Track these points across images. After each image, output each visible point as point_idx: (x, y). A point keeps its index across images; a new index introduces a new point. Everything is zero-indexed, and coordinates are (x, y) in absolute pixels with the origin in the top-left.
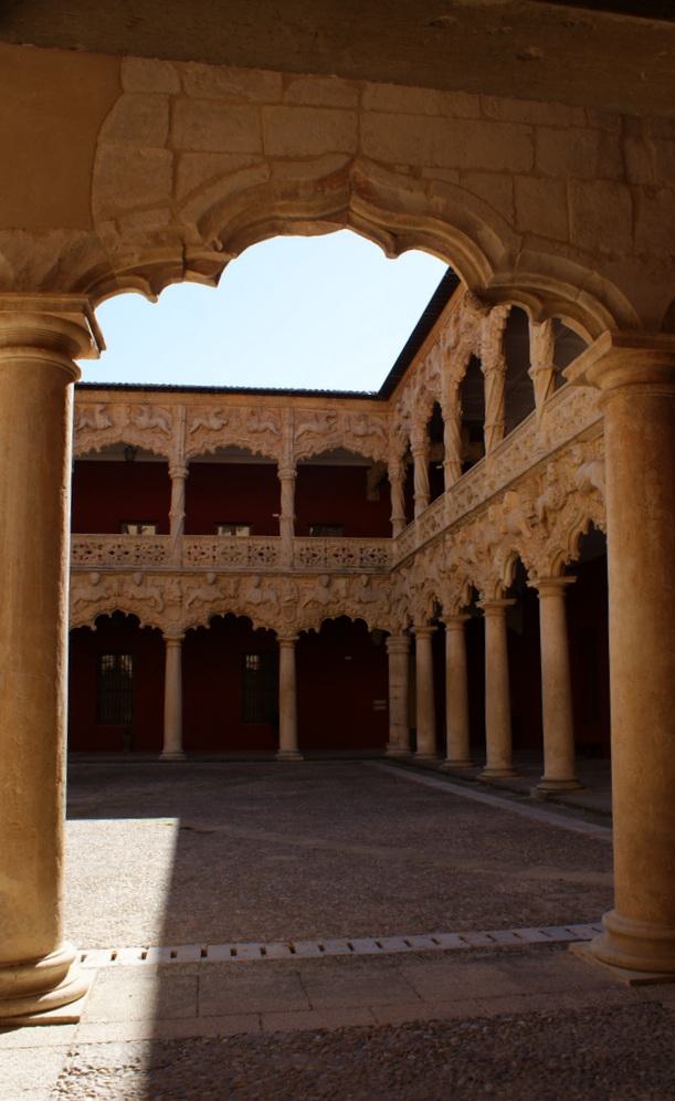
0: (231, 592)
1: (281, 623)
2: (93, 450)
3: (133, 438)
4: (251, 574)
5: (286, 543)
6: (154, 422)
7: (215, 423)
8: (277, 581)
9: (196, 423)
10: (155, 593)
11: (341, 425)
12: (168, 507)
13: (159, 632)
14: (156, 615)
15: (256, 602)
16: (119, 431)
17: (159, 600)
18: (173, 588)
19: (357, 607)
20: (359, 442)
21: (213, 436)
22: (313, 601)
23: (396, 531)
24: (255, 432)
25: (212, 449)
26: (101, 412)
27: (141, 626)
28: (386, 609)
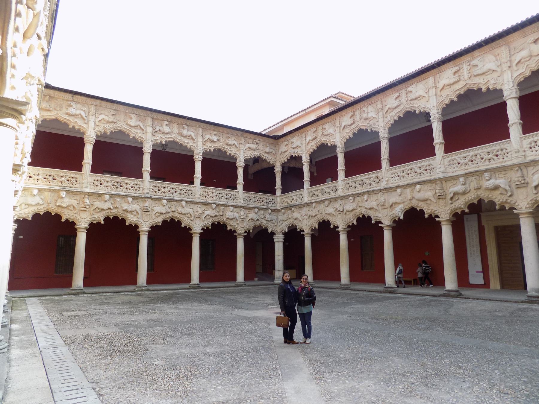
0: (221, 213)
1: (239, 227)
2: (161, 142)
3: (179, 139)
4: (229, 206)
5: (240, 194)
6: (190, 133)
7: (215, 138)
8: (237, 210)
9: (207, 137)
10: (191, 211)
11: (261, 147)
12: (193, 173)
13: (190, 229)
14: (190, 222)
15: (231, 218)
16: (173, 135)
17: (192, 215)
18: (199, 209)
19: (266, 222)
20: (266, 155)
21: (213, 145)
22: (252, 219)
23: (279, 192)
24: (230, 145)
25: (212, 149)
26: (166, 125)
27: (183, 226)
28: (276, 224)
